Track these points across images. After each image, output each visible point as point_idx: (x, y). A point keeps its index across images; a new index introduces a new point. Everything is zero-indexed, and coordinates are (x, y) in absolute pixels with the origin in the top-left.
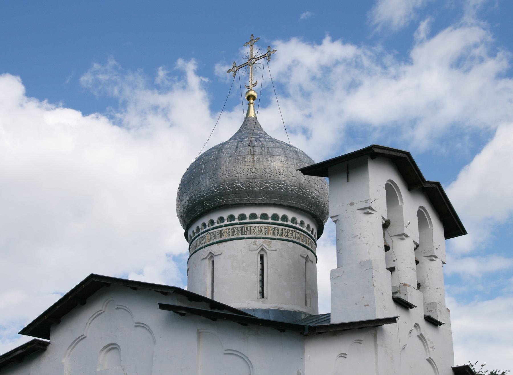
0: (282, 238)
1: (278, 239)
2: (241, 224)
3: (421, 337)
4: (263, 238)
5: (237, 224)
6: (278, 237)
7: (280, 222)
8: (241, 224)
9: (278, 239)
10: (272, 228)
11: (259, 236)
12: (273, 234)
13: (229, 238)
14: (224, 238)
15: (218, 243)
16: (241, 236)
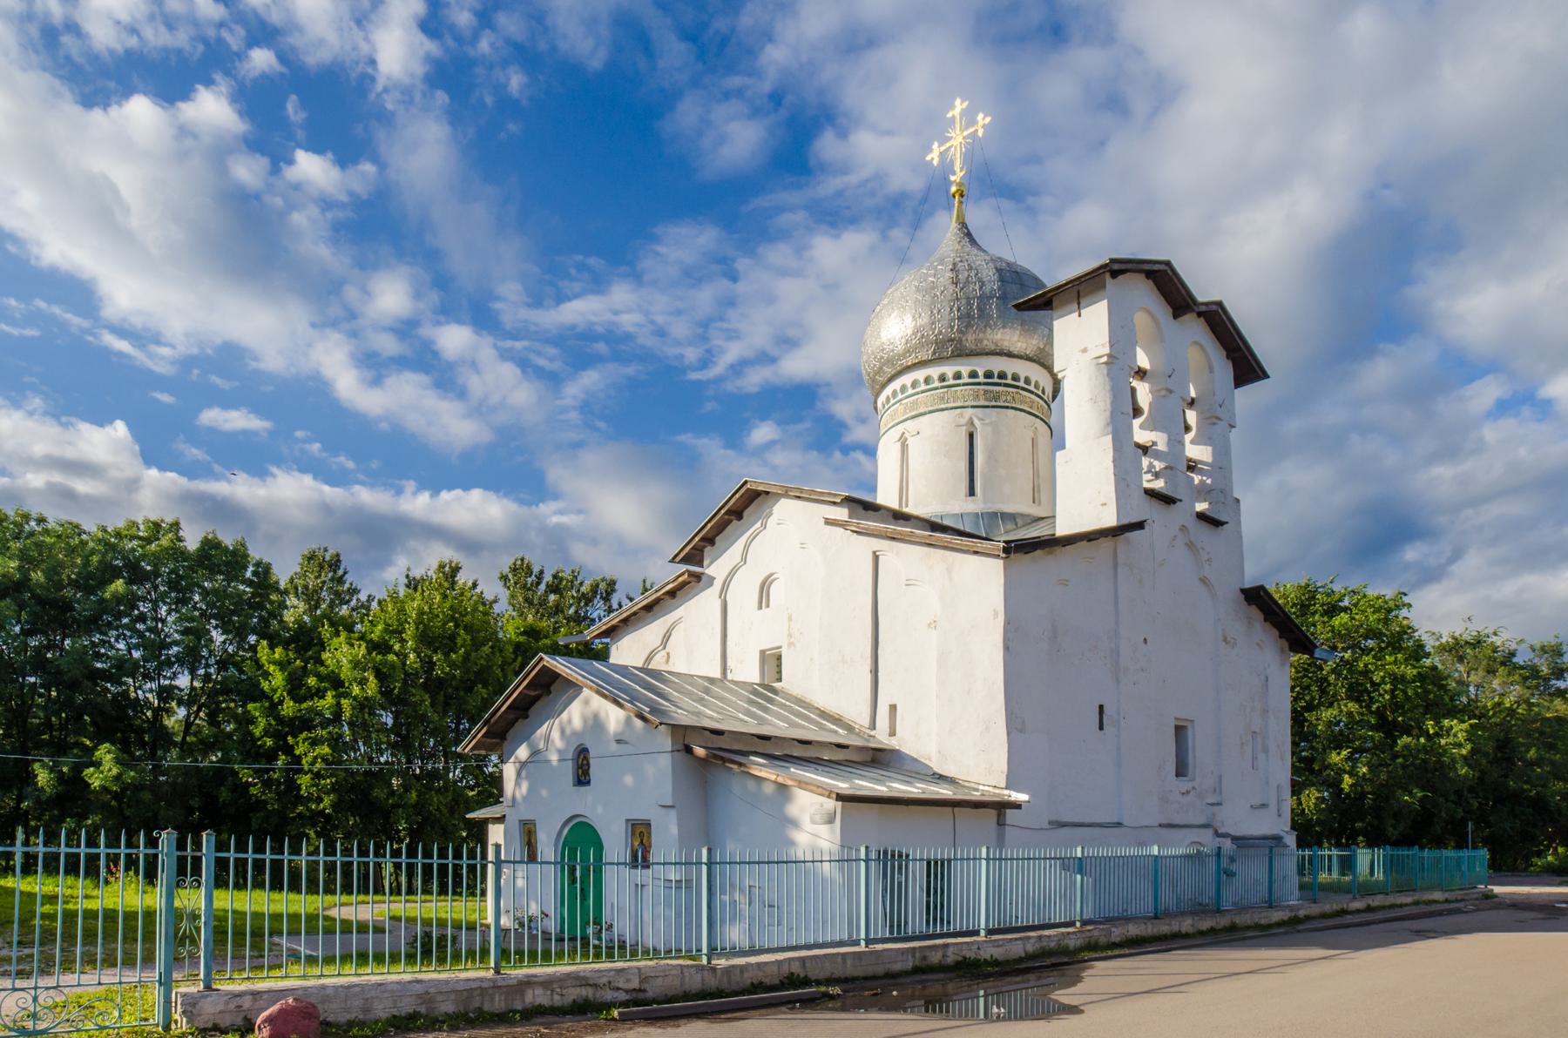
0: (998, 404)
1: (994, 407)
2: (943, 387)
3: (1190, 546)
4: (973, 407)
5: (937, 388)
6: (993, 403)
7: (996, 380)
8: (943, 387)
9: (994, 407)
10: (985, 391)
11: (966, 404)
12: (986, 399)
13: (926, 409)
14: (921, 411)
15: (913, 417)
16: (943, 406)
